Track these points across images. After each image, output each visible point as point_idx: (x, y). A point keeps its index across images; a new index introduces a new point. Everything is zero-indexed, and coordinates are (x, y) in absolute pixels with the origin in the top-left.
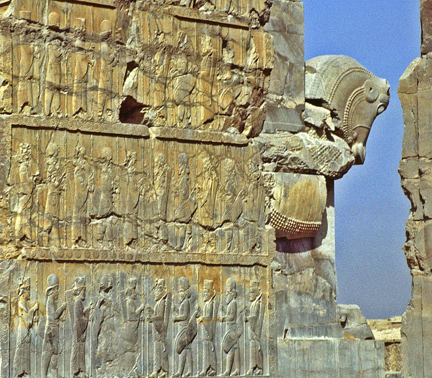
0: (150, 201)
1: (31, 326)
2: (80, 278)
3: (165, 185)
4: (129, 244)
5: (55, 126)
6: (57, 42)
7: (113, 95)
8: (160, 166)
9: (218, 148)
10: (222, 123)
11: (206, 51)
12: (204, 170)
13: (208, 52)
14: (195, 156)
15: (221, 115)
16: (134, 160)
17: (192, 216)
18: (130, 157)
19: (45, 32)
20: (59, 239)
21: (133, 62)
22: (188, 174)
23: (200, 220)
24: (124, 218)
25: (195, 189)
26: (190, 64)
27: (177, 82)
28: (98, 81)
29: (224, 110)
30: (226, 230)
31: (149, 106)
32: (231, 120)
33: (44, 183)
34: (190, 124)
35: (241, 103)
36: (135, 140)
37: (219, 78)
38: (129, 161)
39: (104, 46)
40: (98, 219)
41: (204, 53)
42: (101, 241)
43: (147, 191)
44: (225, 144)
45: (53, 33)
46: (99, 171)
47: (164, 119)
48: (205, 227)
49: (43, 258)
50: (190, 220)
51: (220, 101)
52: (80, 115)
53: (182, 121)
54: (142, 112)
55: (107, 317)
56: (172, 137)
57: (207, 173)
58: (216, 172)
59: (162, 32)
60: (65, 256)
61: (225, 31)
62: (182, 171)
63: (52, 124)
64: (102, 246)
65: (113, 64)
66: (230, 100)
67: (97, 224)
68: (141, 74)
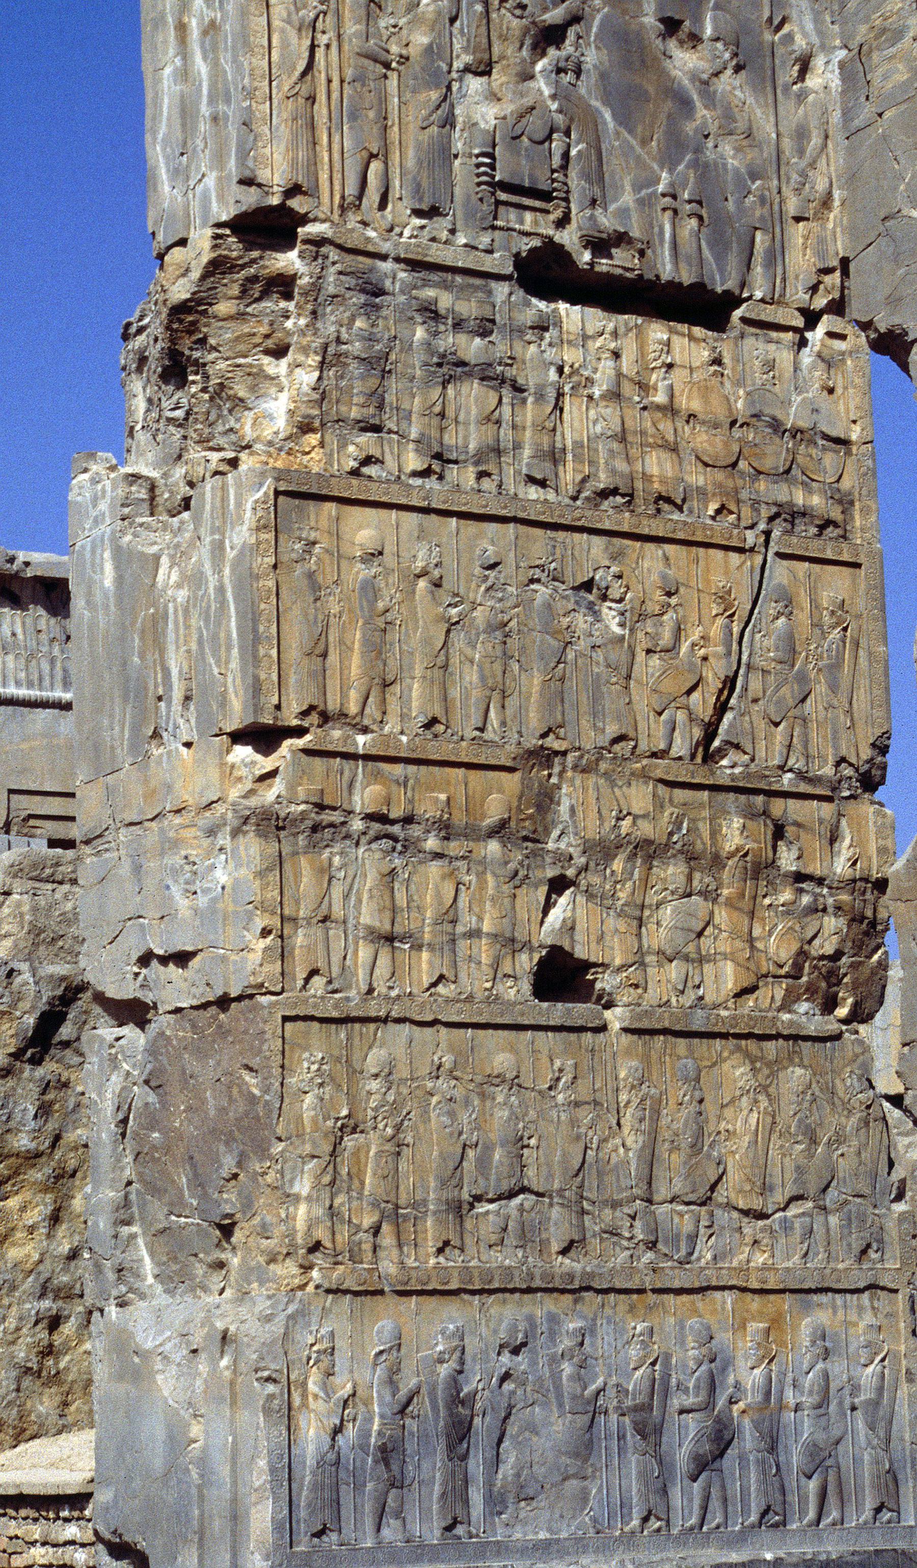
0: (613, 1161)
1: (338, 1430)
2: (451, 1327)
3: (645, 1126)
4: (564, 1252)
5: (382, 1013)
6: (386, 844)
7: (518, 946)
8: (633, 1087)
9: (770, 1046)
10: (779, 993)
11: (733, 848)
12: (738, 1093)
13: (737, 850)
14: (714, 1064)
15: (774, 977)
16: (570, 1076)
17: (713, 1188)
18: (561, 1070)
19: (357, 825)
20: (400, 1246)
21: (563, 877)
22: (701, 1101)
23: (732, 1195)
24: (551, 1197)
25: (719, 1133)
26: (697, 876)
27: (667, 913)
28: (480, 919)
29: (781, 967)
30: (795, 1216)
31: (602, 965)
32: (800, 986)
33: (362, 1132)
34: (701, 998)
35: (821, 952)
36: (573, 1037)
37: (767, 901)
38: (558, 1079)
39: (493, 847)
40: (491, 1201)
43: (606, 1140)
44: (787, 1038)
45: (376, 826)
46: (488, 1103)
47: (640, 991)
48: (746, 1213)
50: (710, 1198)
51: (772, 950)
52: (440, 989)
53: (682, 992)
54: (589, 977)
56: (658, 1026)
57: (744, 1099)
58: (768, 1095)
59: (629, 814)
60: (413, 1281)
61: (778, 807)
63: (374, 1009)
65: (517, 882)
66: (795, 947)
67: (487, 1212)
68: (581, 899)
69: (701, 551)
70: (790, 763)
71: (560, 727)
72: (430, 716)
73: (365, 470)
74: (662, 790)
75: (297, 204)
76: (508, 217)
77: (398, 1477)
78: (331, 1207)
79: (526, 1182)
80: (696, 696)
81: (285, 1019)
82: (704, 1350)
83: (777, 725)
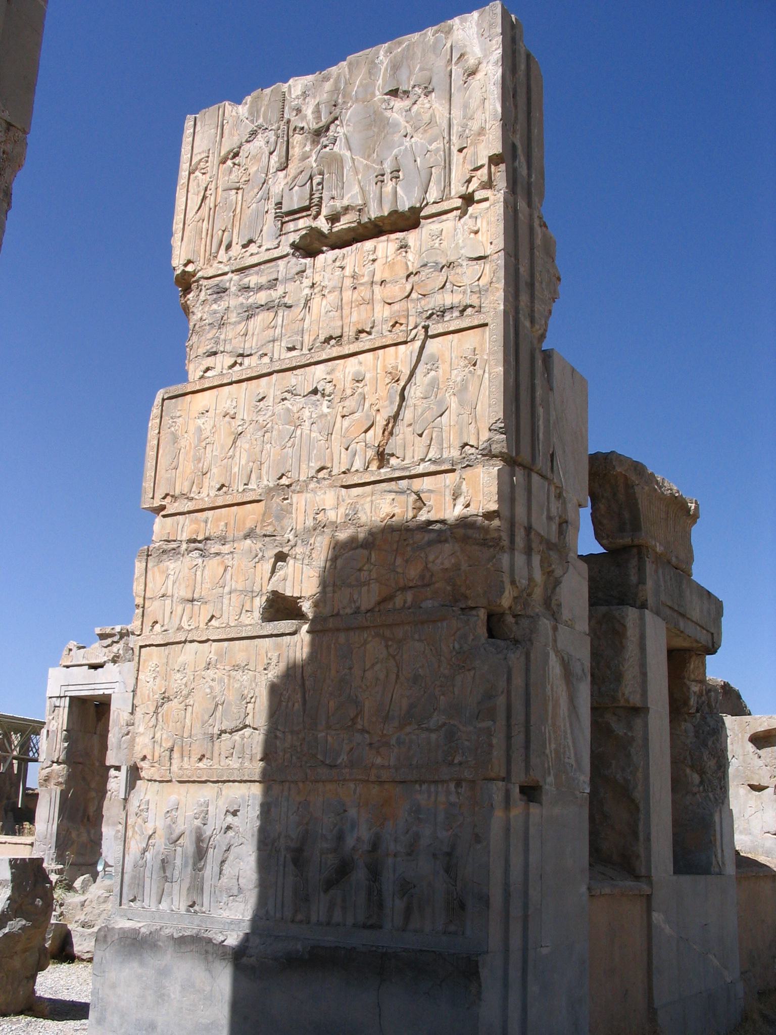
1: (145, 851)
2: (202, 800)
5: (183, 639)
11: (385, 514)
19: (184, 546)
20: (182, 757)
24: (260, 730)
34: (359, 608)
41: (382, 518)
42: (230, 759)
49: (161, 779)
52: (213, 622)
55: (234, 845)
60: (185, 776)
61: (417, 484)
64: (234, 763)
65: (257, 560)
69: (381, 352)
70: (430, 456)
72: (221, 484)
75: (190, 268)
76: (291, 226)
78: (153, 738)
79: (247, 723)
80: (371, 432)
81: (141, 647)
83: (420, 435)
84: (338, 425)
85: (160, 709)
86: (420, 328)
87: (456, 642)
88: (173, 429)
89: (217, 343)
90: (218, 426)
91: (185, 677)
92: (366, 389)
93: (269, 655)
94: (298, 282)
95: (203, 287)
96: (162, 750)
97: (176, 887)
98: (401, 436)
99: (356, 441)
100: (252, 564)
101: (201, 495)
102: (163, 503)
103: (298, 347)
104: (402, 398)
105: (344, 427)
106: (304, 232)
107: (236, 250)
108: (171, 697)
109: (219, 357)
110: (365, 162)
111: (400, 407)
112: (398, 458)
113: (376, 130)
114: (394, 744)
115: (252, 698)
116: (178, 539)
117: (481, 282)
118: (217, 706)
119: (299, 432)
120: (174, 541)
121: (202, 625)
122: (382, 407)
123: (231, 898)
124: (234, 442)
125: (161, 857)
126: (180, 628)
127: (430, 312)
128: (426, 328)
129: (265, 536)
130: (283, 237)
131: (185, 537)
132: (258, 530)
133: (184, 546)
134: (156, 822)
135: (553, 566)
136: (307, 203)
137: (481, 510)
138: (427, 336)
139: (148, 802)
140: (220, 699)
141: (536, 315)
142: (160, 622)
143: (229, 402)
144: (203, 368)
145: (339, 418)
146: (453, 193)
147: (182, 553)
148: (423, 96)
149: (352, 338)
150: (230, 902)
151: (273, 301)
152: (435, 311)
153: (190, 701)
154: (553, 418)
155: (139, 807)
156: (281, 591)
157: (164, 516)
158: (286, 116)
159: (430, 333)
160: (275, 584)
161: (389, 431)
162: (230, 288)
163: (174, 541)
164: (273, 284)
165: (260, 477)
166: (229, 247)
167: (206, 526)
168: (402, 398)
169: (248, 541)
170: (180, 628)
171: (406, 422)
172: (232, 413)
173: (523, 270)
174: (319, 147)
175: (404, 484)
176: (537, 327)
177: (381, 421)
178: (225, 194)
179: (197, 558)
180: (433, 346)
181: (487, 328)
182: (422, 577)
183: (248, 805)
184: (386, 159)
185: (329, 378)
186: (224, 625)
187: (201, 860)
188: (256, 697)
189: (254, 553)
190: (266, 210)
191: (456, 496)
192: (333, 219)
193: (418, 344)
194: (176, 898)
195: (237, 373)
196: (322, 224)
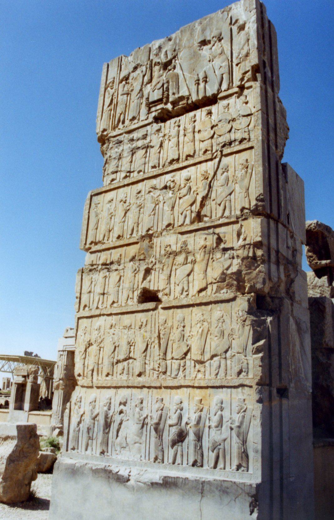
11: (201, 246)
12: (197, 322)
13: (202, 246)
19: (100, 267)
20: (98, 374)
38: (142, 325)
46: (123, 334)
61: (217, 230)
62: (178, 326)
65: (136, 272)
66: (220, 271)
71: (152, 227)
73: (112, 183)
74: (180, 236)
76: (153, 109)
77: (91, 436)
79: (131, 356)
82: (178, 406)
83: (220, 205)
84: (177, 202)
85: (87, 349)
86: (219, 152)
87: (240, 311)
88: (95, 210)
89: (117, 167)
90: (117, 206)
91: (99, 333)
92: (191, 184)
93: (142, 321)
94: (157, 135)
95: (111, 142)
96: (88, 371)
97: (94, 442)
98: (209, 206)
99: (187, 209)
100: (133, 274)
101: (109, 241)
102: (90, 246)
103: (157, 165)
104: (210, 187)
105: (180, 203)
106: (160, 111)
107: (127, 122)
108: (93, 343)
109: (118, 174)
110: (189, 75)
111: (209, 191)
112: (208, 217)
113: (195, 60)
114: (208, 366)
115: (133, 343)
116: (98, 263)
117: (250, 127)
118: (115, 347)
119: (157, 207)
120: (95, 265)
121: (109, 306)
122: (200, 192)
123: (122, 449)
124: (126, 213)
125: (87, 426)
126: (97, 308)
127: (223, 143)
128: (221, 152)
129: (140, 260)
130: (150, 115)
131: (101, 262)
132: (136, 258)
133: (100, 267)
134: (86, 408)
135: (290, 272)
136: (161, 97)
137: (252, 241)
138: (222, 155)
139: (81, 398)
140: (117, 344)
141: (278, 144)
142: (88, 305)
143: (123, 195)
144: (110, 179)
145: (178, 199)
146: (234, 85)
147: (99, 270)
148: (217, 41)
149: (184, 159)
150: (122, 451)
151: (145, 145)
152: (226, 143)
153: (102, 345)
154: (288, 197)
155: (76, 400)
156: (147, 287)
157: (91, 253)
158: (151, 58)
159: (224, 153)
160: (145, 284)
161: (202, 205)
162: (124, 141)
163: (95, 265)
164: (145, 137)
165: (138, 231)
166: (123, 122)
167: (111, 256)
168: (210, 187)
169: (132, 263)
170: (97, 308)
171: (212, 198)
172: (124, 200)
173: (271, 121)
174: (167, 71)
175: (211, 231)
176: (279, 150)
177: (199, 199)
178: (122, 97)
179: (106, 272)
180: (225, 160)
181: (253, 150)
182: (220, 278)
183: (131, 399)
184: (200, 73)
185: (172, 179)
186: (119, 306)
187: (107, 428)
188: (135, 343)
189: (134, 268)
190: (141, 102)
191: (239, 235)
192: (174, 103)
193: (217, 160)
194: (94, 448)
195: (127, 181)
196: (169, 106)
